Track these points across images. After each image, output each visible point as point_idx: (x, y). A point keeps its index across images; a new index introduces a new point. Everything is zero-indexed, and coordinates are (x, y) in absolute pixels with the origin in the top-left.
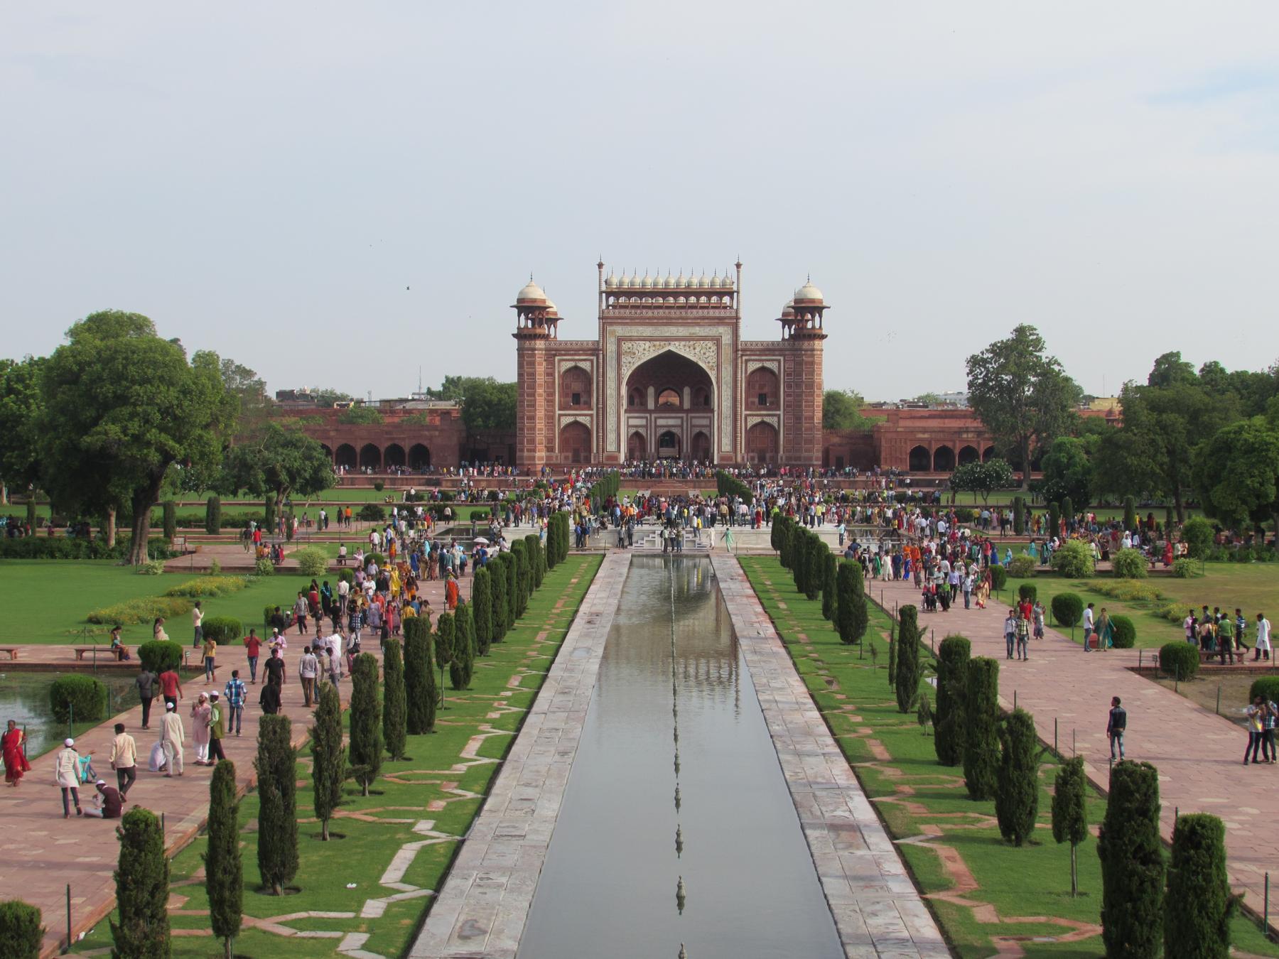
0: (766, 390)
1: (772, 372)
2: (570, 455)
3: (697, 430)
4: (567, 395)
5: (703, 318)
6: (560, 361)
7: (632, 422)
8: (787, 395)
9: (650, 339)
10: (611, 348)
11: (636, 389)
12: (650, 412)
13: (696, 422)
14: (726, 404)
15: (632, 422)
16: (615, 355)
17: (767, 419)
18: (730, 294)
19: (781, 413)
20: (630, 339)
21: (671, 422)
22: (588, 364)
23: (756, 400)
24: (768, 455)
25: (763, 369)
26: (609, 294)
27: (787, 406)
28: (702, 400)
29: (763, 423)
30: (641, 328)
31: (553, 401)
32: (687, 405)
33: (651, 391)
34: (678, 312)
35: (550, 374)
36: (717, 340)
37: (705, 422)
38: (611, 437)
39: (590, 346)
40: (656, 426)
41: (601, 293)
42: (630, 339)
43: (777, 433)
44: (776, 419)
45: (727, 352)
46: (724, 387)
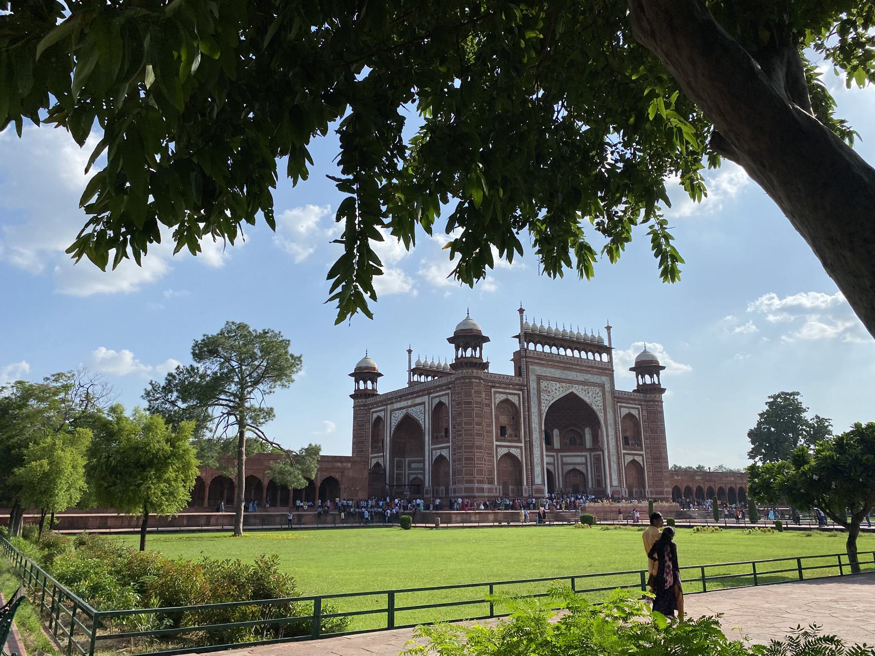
0: (628, 434)
3: (571, 467)
6: (496, 392)
8: (646, 439)
10: (533, 385)
14: (612, 443)
19: (643, 453)
20: (546, 378)
22: (516, 397)
27: (647, 448)
30: (553, 370)
36: (602, 386)
38: (537, 470)
42: (546, 378)
43: (642, 469)
44: (641, 458)
45: (608, 396)
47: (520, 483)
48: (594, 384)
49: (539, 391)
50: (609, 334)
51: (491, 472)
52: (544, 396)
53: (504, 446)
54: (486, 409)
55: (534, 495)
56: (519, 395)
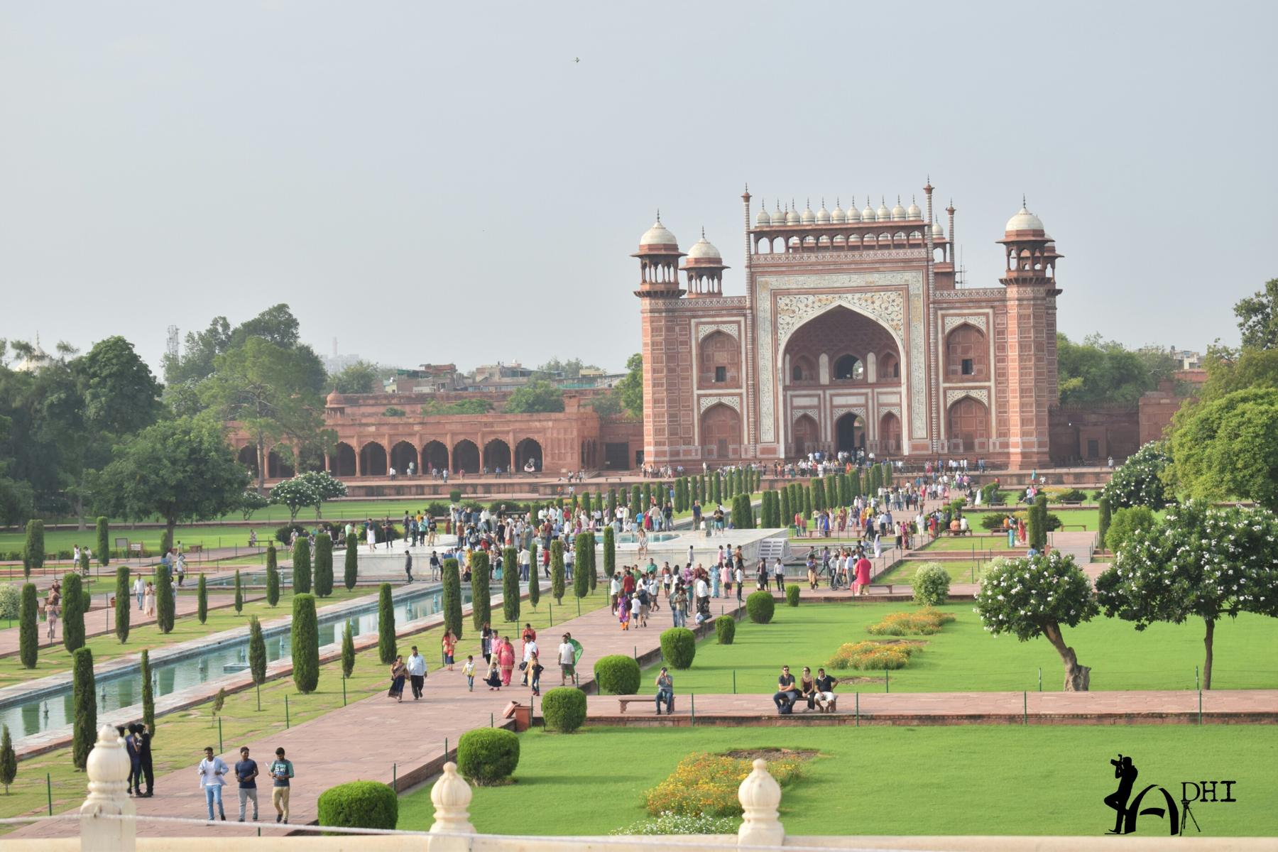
0: (971, 355)
1: (979, 331)
2: (715, 447)
3: (884, 411)
4: (708, 370)
5: (883, 262)
6: (698, 324)
7: (799, 402)
9: (815, 292)
10: (764, 304)
11: (803, 357)
12: (824, 388)
13: (885, 399)
14: (920, 375)
15: (799, 402)
16: (768, 315)
17: (974, 394)
18: (920, 228)
19: (992, 384)
20: (788, 292)
21: (852, 400)
22: (735, 326)
23: (959, 368)
24: (977, 441)
25: (966, 326)
26: (759, 235)
28: (891, 370)
29: (967, 398)
30: (801, 278)
31: (689, 378)
32: (872, 378)
33: (824, 360)
34: (850, 254)
35: (686, 343)
36: (904, 290)
37: (894, 399)
38: (767, 423)
39: (736, 304)
40: (832, 407)
41: (749, 233)
43: (987, 411)
45: (919, 304)
46: (914, 352)
47: (741, 442)
48: (885, 288)
49: (775, 313)
50: (930, 198)
51: (689, 428)
52: (784, 319)
53: (711, 395)
54: (682, 349)
55: (759, 456)
56: (739, 323)
